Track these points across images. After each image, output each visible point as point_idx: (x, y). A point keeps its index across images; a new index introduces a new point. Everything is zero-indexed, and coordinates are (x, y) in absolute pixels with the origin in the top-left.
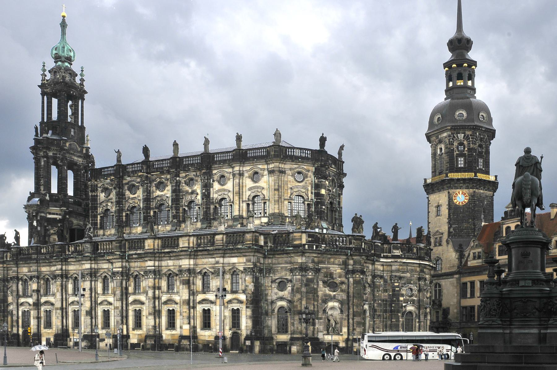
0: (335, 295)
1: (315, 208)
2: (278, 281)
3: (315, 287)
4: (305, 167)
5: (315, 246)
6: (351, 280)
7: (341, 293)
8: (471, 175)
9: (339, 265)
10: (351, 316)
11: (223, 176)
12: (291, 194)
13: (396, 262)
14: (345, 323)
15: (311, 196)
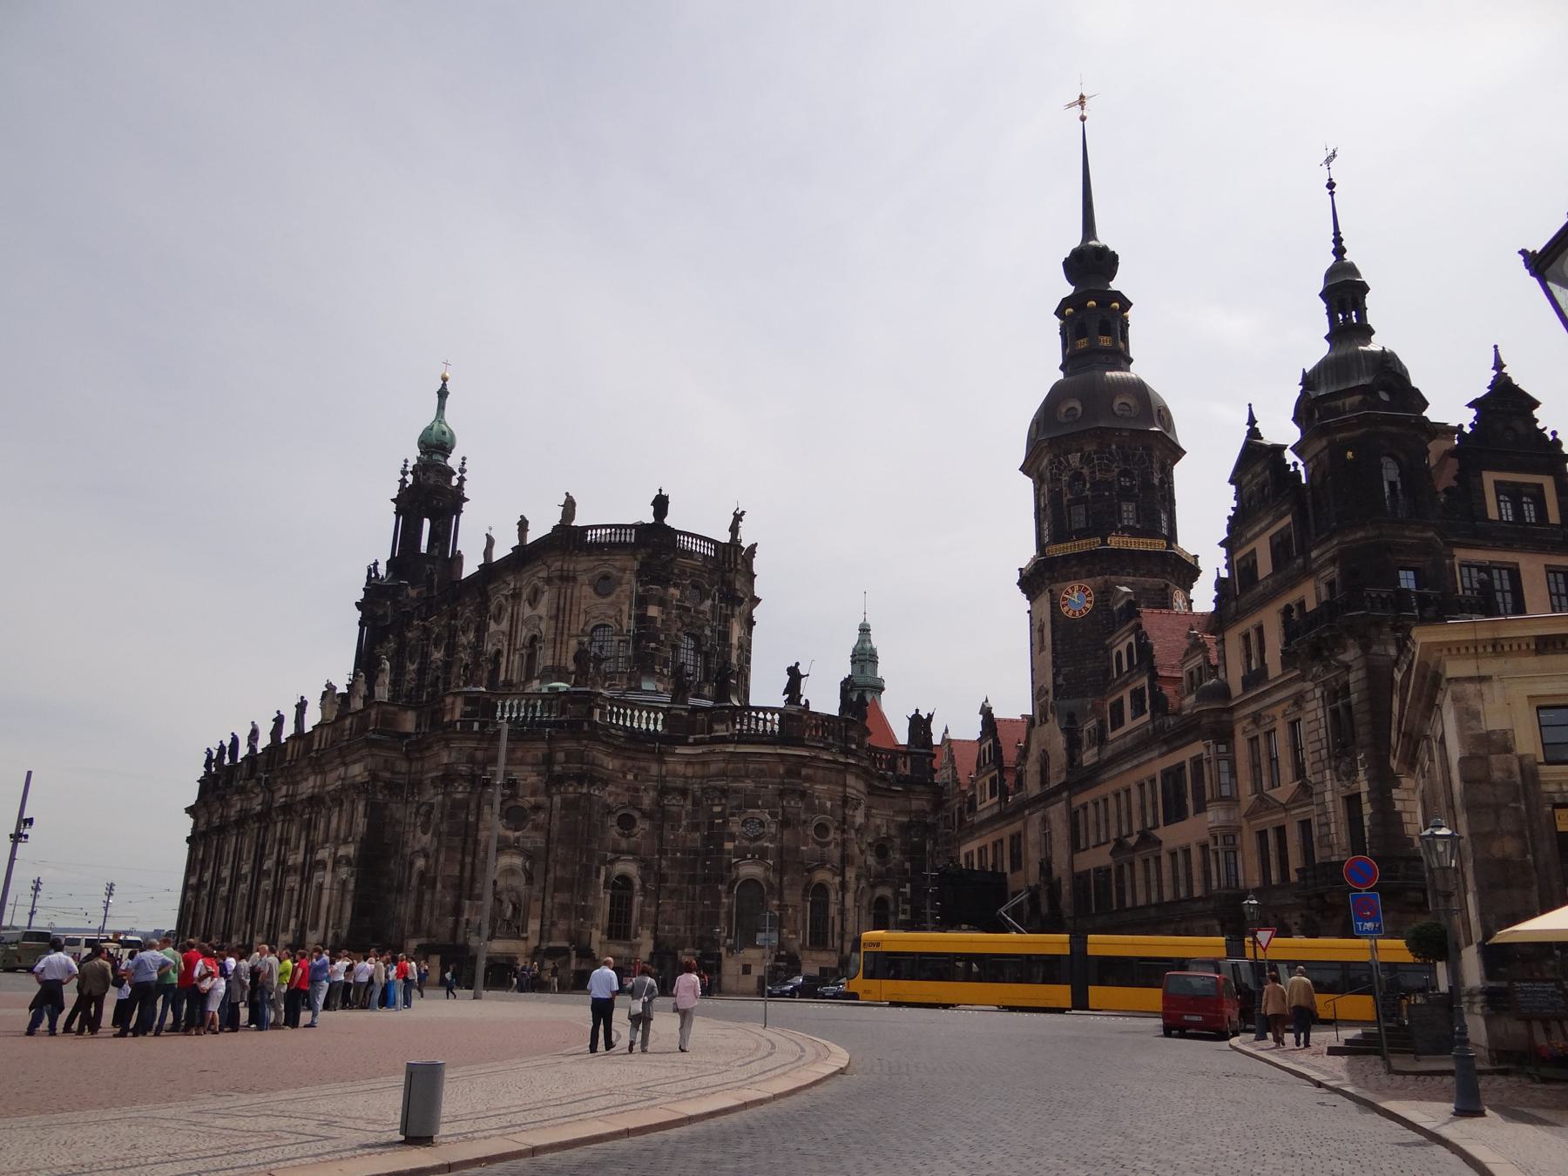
0: (517, 839)
1: (635, 649)
2: (423, 810)
3: (472, 819)
4: (617, 564)
5: (476, 726)
6: (557, 799)
7: (533, 834)
8: (1094, 543)
9: (533, 765)
10: (550, 890)
11: (500, 608)
12: (586, 623)
13: (712, 752)
14: (536, 908)
15: (629, 624)
